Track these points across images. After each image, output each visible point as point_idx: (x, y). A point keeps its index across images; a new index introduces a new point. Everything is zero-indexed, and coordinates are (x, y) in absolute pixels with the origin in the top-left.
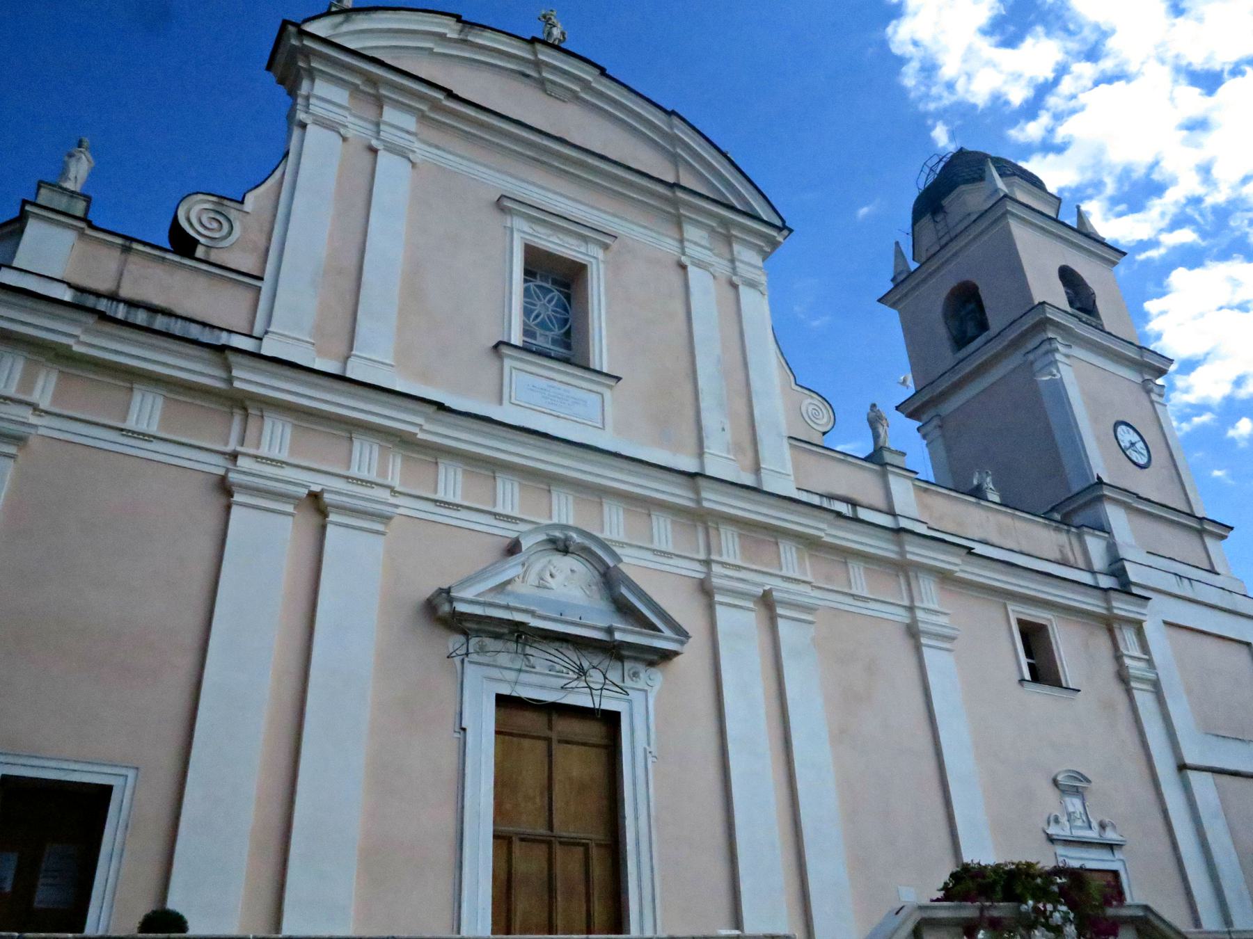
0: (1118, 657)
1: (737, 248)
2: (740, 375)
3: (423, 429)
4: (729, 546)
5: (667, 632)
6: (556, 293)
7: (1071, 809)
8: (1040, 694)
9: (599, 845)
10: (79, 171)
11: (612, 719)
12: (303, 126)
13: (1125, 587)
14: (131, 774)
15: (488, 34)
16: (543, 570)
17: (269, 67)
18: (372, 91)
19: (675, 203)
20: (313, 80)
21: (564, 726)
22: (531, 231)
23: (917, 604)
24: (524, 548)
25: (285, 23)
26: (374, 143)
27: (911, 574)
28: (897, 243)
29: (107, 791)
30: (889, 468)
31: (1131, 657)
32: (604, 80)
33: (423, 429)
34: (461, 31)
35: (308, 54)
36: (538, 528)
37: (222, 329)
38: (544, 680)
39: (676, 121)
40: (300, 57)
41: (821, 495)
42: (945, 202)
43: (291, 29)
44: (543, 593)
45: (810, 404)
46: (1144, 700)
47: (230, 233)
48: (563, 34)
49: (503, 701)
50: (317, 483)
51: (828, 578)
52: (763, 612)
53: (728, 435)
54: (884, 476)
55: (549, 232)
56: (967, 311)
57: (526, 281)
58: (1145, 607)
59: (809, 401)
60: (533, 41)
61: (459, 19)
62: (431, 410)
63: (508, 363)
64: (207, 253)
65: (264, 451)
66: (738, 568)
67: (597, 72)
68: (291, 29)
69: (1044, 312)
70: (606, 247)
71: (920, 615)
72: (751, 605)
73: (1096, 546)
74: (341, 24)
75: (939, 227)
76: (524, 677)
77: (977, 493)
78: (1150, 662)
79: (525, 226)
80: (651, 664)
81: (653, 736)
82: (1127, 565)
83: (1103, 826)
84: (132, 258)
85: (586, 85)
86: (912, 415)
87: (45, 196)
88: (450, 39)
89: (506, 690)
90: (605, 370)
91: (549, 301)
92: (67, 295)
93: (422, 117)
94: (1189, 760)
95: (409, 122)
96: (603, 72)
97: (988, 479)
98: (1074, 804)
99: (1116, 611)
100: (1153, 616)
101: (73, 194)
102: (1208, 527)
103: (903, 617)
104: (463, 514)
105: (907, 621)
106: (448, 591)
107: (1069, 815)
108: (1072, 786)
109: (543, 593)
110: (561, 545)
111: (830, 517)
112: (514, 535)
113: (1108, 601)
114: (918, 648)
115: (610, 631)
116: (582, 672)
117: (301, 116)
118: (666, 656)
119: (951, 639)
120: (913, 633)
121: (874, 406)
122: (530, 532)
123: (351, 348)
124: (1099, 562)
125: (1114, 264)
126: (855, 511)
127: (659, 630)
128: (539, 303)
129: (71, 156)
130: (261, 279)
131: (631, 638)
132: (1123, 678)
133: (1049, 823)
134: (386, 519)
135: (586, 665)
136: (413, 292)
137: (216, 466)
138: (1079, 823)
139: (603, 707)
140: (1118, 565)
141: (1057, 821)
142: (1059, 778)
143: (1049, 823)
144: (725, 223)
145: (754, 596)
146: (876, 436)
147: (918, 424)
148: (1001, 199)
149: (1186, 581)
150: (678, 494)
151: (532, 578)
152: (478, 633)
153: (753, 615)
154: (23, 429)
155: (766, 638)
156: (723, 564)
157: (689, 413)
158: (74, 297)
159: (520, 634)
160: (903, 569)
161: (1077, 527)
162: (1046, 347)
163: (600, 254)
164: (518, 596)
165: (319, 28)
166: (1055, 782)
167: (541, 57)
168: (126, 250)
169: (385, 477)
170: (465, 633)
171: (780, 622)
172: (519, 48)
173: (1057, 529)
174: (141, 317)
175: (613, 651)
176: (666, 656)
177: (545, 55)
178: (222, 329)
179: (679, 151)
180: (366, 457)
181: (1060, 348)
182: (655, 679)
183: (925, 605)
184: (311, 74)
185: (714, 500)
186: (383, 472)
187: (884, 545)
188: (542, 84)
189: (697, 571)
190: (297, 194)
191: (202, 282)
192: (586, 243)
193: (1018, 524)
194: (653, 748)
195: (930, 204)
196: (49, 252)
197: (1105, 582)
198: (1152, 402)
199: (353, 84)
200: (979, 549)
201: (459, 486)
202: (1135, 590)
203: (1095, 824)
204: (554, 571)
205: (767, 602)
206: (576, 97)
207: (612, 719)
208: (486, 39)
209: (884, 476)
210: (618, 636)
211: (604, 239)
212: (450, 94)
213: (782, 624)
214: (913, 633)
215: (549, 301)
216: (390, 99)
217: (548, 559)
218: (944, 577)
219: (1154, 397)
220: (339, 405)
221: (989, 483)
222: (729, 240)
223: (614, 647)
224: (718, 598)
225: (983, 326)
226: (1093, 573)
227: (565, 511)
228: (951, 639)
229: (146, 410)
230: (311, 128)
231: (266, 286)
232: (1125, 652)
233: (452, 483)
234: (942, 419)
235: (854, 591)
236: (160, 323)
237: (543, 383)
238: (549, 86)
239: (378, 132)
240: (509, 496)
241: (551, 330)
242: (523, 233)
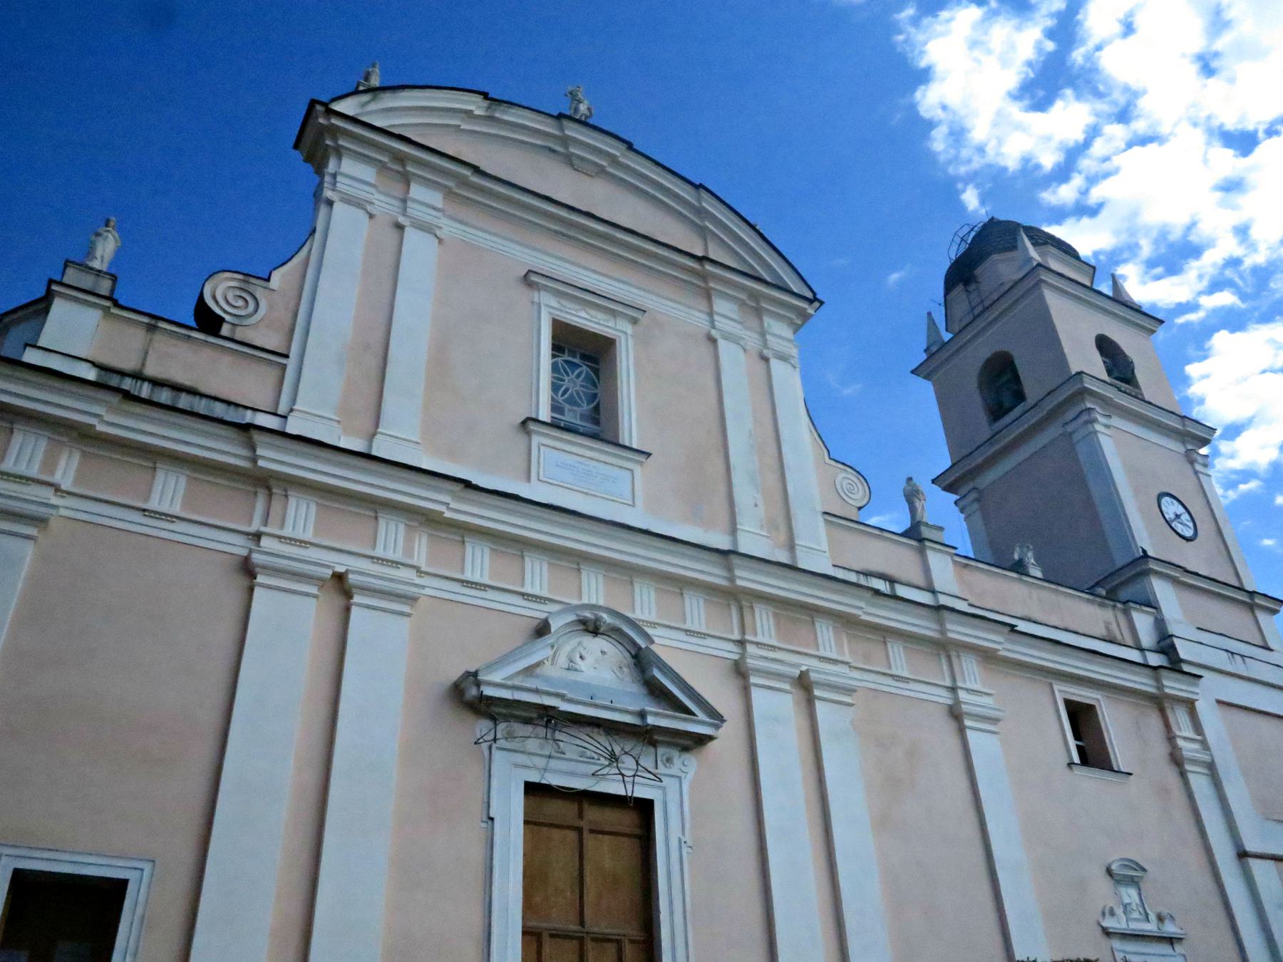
0: (1171, 738)
1: (768, 321)
2: (772, 450)
3: (450, 508)
4: (764, 625)
5: (701, 716)
6: (584, 367)
7: (1127, 900)
8: (1089, 779)
9: (632, 942)
10: (106, 249)
11: (645, 808)
12: (330, 203)
13: (1175, 664)
14: (147, 867)
15: (514, 110)
16: (573, 650)
17: (296, 146)
18: (703, 285)
19: (704, 277)
20: (340, 157)
21: (594, 814)
22: (556, 305)
23: (960, 684)
24: (553, 630)
25: (313, 103)
26: (401, 220)
27: (953, 654)
28: (929, 314)
29: (122, 884)
30: (927, 544)
31: (1185, 739)
32: (631, 155)
33: (450, 508)
34: (488, 108)
35: (335, 132)
36: (568, 608)
37: (247, 408)
38: (575, 766)
39: (704, 195)
40: (326, 135)
41: (858, 572)
42: (978, 272)
43: (319, 108)
44: (572, 676)
45: (844, 478)
46: (1200, 783)
47: (256, 310)
48: (589, 109)
49: (532, 789)
50: (340, 564)
51: (867, 658)
52: (800, 694)
53: (761, 511)
54: (922, 552)
55: (577, 307)
56: (1002, 383)
57: (554, 356)
58: (1197, 685)
59: (844, 475)
60: (560, 117)
61: (485, 96)
62: (458, 488)
63: (536, 440)
64: (233, 331)
65: (288, 532)
66: (773, 648)
67: (623, 147)
68: (319, 108)
69: (1082, 381)
70: (635, 321)
71: (962, 695)
72: (787, 687)
73: (1143, 622)
74: (369, 102)
75: (973, 296)
76: (553, 764)
77: (1019, 568)
78: (1205, 744)
79: (553, 302)
80: (685, 749)
81: (687, 826)
82: (1176, 641)
83: (1160, 919)
84: (158, 337)
85: (614, 160)
86: (950, 488)
87: (72, 276)
89: (534, 777)
90: (635, 446)
91: (578, 376)
92: (91, 374)
93: (449, 194)
94: (1250, 847)
95: (436, 198)
96: (630, 147)
97: (1030, 554)
98: (1130, 895)
99: (1167, 690)
100: (1206, 693)
101: (99, 273)
102: (1258, 601)
103: (945, 698)
104: (491, 595)
105: (950, 702)
106: (475, 674)
107: (1125, 906)
108: (1127, 875)
109: (572, 676)
110: (591, 628)
111: (868, 595)
112: (543, 616)
113: (1158, 680)
114: (962, 730)
115: (642, 715)
116: (613, 758)
117: (328, 193)
118: (702, 740)
119: (995, 720)
120: (955, 714)
121: (910, 479)
122: (559, 613)
123: (377, 425)
124: (1147, 636)
125: (1153, 332)
126: (893, 588)
127: (694, 714)
128: (566, 378)
129: (98, 235)
130: (287, 356)
131: (665, 720)
132: (1177, 760)
133: (1104, 914)
134: (412, 600)
135: (617, 750)
136: (439, 366)
137: (239, 546)
138: (1135, 915)
139: (635, 795)
140: (1168, 641)
141: (1112, 913)
142: (1113, 867)
143: (1104, 914)
144: (754, 295)
145: (788, 677)
146: (913, 510)
147: (955, 497)
148: (1034, 268)
149: (1237, 658)
150: (712, 573)
151: (562, 660)
152: (507, 718)
153: (789, 698)
154: (42, 510)
155: (805, 723)
156: (757, 644)
157: (722, 488)
158: (99, 376)
159: (549, 718)
160: (943, 648)
161: (1125, 603)
162: (1085, 417)
163: (629, 328)
164: (547, 680)
165: (346, 107)
166: (1109, 872)
167: (567, 132)
168: (151, 328)
169: (412, 556)
170: (494, 719)
171: (818, 704)
172: (547, 125)
173: (1101, 605)
174: (164, 396)
175: (645, 735)
176: (702, 740)
177: (572, 131)
178: (247, 408)
179: (707, 224)
180: (392, 537)
181: (1100, 419)
182: (688, 766)
183: (968, 685)
184: (339, 152)
185: (747, 578)
186: (409, 550)
187: (1144, 681)
188: (569, 160)
189: (731, 652)
190: (323, 270)
191: (227, 359)
192: (615, 317)
193: (1062, 599)
194: (687, 838)
195: (962, 273)
196: (74, 332)
197: (1155, 659)
198: (1196, 473)
199: (446, 186)
200: (1023, 626)
201: (703, 617)
202: (1186, 668)
203: (1152, 917)
204: (584, 654)
205: (804, 684)
206: (601, 171)
207: (645, 808)
208: (512, 116)
209: (922, 552)
210: (651, 720)
211: (635, 313)
212: (476, 170)
213: (819, 705)
214: (955, 714)
215: (578, 376)
216: (768, 310)
217: (577, 640)
218: (988, 657)
219: (1198, 467)
220: (365, 484)
221: (1030, 558)
222: (758, 312)
223: (647, 732)
224: (753, 680)
225: (1020, 396)
226: (1141, 650)
227: (594, 591)
228: (995, 720)
229: (169, 490)
230: (338, 207)
231: (291, 363)
232: (1178, 733)
233: (479, 562)
234: (980, 492)
235: (894, 671)
236: (184, 401)
237: (570, 459)
238: (576, 162)
239: (405, 210)
240: (538, 576)
241: (579, 406)
242: (550, 308)
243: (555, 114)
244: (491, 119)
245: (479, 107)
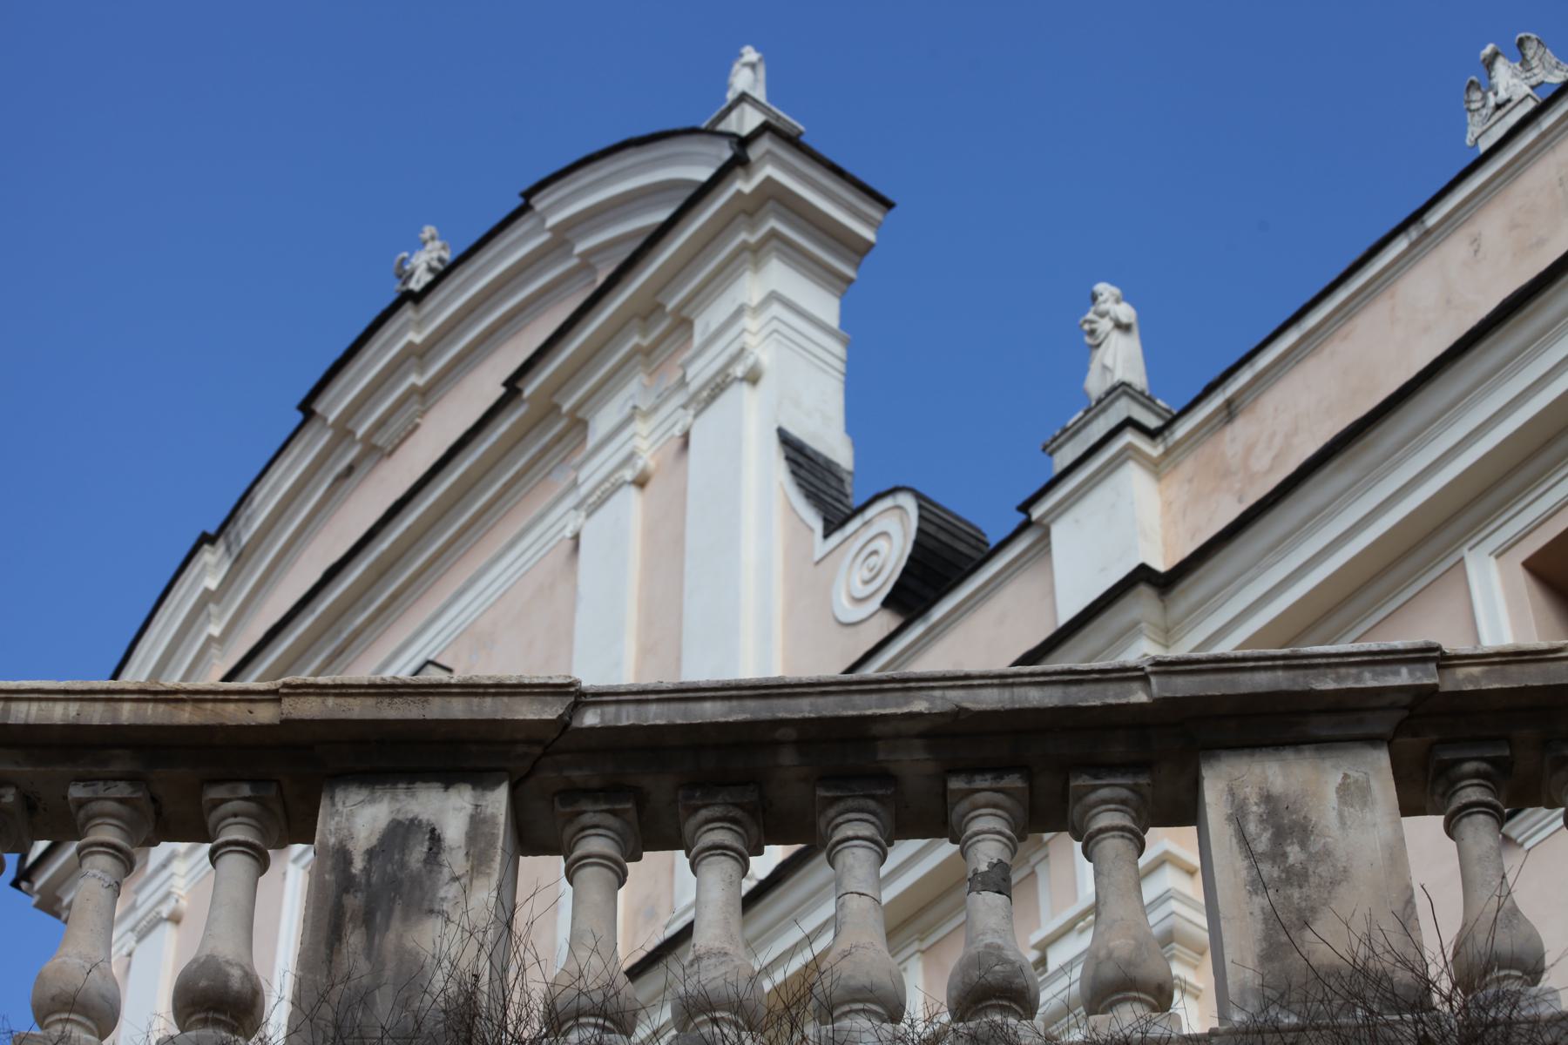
32: (431, 303)
39: (540, 203)
60: (307, 408)
61: (207, 539)
67: (408, 312)
85: (418, 355)
88: (227, 582)
144: (647, 311)
177: (333, 406)
179: (581, 247)
238: (380, 440)
243: (299, 417)
244: (240, 561)
245: (218, 564)
